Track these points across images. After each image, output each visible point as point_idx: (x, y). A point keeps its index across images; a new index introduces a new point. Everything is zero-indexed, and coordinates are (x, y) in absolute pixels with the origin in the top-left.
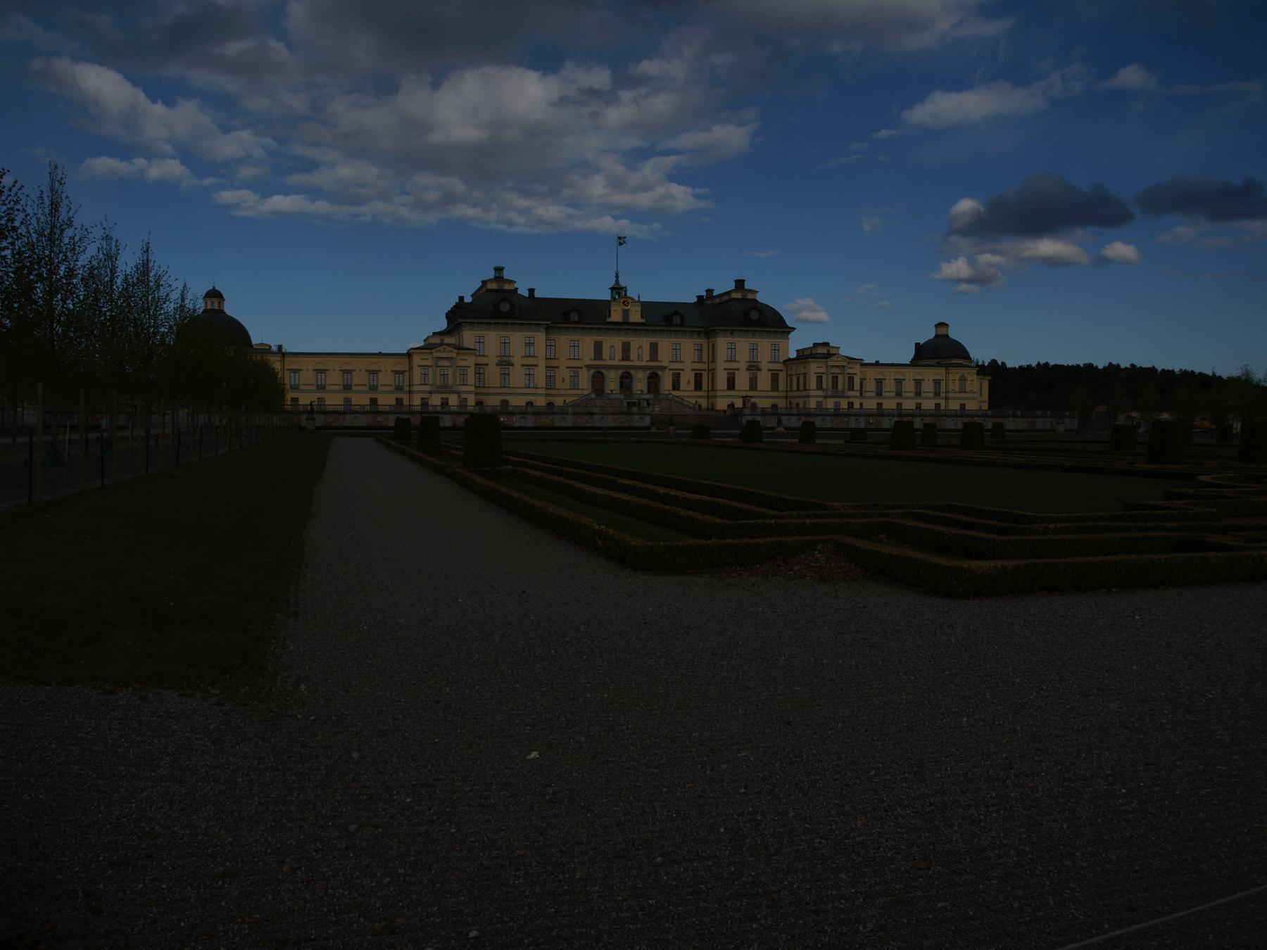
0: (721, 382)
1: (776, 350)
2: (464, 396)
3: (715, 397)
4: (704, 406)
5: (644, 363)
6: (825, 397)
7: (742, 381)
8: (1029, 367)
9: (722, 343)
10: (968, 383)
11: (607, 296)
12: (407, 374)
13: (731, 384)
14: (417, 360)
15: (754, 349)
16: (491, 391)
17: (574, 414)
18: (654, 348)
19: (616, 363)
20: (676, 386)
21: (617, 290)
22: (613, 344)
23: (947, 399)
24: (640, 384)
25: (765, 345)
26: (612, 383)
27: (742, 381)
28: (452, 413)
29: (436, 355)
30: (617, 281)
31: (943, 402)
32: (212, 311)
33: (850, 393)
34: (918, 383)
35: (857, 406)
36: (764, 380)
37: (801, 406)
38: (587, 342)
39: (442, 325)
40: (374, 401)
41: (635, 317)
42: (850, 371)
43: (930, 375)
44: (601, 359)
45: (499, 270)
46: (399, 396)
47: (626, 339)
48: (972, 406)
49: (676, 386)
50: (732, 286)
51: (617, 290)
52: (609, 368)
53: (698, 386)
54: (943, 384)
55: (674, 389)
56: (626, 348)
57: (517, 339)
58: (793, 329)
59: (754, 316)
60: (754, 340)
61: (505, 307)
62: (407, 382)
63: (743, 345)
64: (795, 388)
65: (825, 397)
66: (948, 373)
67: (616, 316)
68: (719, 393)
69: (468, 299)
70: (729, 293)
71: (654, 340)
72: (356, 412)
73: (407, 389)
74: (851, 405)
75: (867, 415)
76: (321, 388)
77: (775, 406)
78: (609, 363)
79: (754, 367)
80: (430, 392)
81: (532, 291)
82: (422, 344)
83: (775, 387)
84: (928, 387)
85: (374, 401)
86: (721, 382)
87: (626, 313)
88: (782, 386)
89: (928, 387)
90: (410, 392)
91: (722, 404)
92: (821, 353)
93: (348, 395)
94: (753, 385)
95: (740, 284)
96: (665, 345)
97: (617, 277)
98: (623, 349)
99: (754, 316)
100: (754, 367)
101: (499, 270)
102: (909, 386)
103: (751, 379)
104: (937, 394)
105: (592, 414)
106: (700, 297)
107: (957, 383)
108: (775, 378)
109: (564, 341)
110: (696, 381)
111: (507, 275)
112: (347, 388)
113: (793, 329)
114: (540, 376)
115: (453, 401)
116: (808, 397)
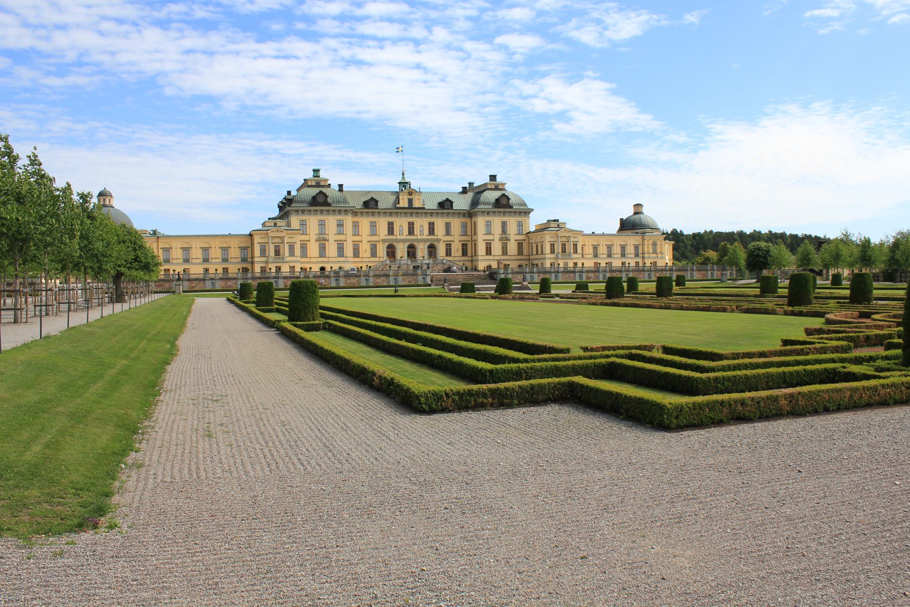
0: (481, 250)
1: (520, 225)
2: (292, 265)
3: (477, 260)
4: (469, 266)
5: (425, 237)
6: (557, 258)
7: (497, 248)
8: (699, 234)
9: (481, 221)
10: (658, 247)
11: (396, 188)
12: (250, 250)
13: (489, 251)
14: (257, 239)
15: (504, 224)
16: (312, 260)
17: (375, 276)
18: (431, 227)
19: (404, 237)
21: (403, 184)
22: (401, 223)
23: (643, 258)
24: (422, 251)
25: (512, 222)
26: (401, 251)
27: (497, 248)
28: (285, 278)
29: (271, 235)
30: (403, 178)
31: (640, 260)
32: (105, 206)
33: (575, 256)
34: (623, 248)
35: (579, 265)
36: (512, 248)
37: (540, 266)
38: (382, 223)
39: (276, 212)
40: (226, 270)
41: (416, 204)
42: (575, 240)
43: (631, 240)
44: (393, 234)
45: (316, 171)
46: (245, 265)
47: (411, 220)
48: (661, 264)
49: (448, 253)
50: (487, 180)
51: (403, 184)
52: (398, 241)
53: (464, 253)
54: (640, 247)
55: (447, 255)
56: (411, 226)
57: (331, 221)
58: (532, 210)
60: (504, 219)
61: (321, 199)
62: (250, 256)
63: (497, 221)
64: (535, 252)
65: (557, 258)
66: (643, 240)
67: (404, 203)
68: (480, 258)
69: (294, 193)
70: (485, 185)
71: (432, 220)
72: (212, 279)
73: (250, 260)
74: (576, 264)
75: (588, 272)
76: (186, 261)
77: (520, 266)
78: (399, 237)
79: (505, 240)
80: (267, 262)
81: (341, 186)
82: (260, 227)
83: (520, 252)
84: (630, 250)
85: (226, 270)
86: (481, 250)
87: (410, 201)
88: (525, 252)
89: (630, 250)
90: (252, 263)
91: (481, 266)
92: (552, 225)
93: (207, 266)
94: (505, 251)
95: (493, 178)
96: (440, 224)
97: (403, 174)
98: (409, 228)
99: (504, 202)
100: (505, 240)
101: (316, 171)
102: (617, 250)
103: (503, 248)
104: (637, 255)
105: (387, 276)
106: (464, 188)
107: (651, 247)
108: (520, 245)
109: (365, 222)
110: (463, 249)
111: (322, 175)
112: (206, 260)
113: (532, 210)
114: (349, 250)
115: (285, 269)
116: (545, 259)
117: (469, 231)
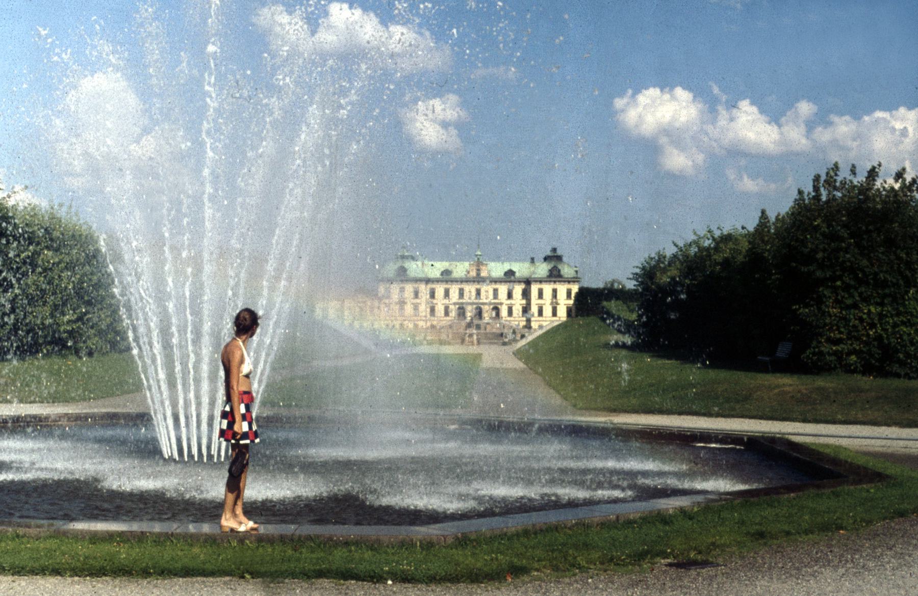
0: (534, 309)
7: (547, 311)
9: (534, 288)
13: (540, 313)
15: (555, 291)
18: (496, 291)
20: (510, 312)
22: (470, 289)
27: (547, 311)
38: (454, 290)
41: (484, 274)
49: (510, 312)
56: (478, 292)
57: (409, 288)
59: (555, 273)
63: (548, 289)
96: (503, 289)
109: (440, 290)
114: (424, 309)
117: (526, 294)
